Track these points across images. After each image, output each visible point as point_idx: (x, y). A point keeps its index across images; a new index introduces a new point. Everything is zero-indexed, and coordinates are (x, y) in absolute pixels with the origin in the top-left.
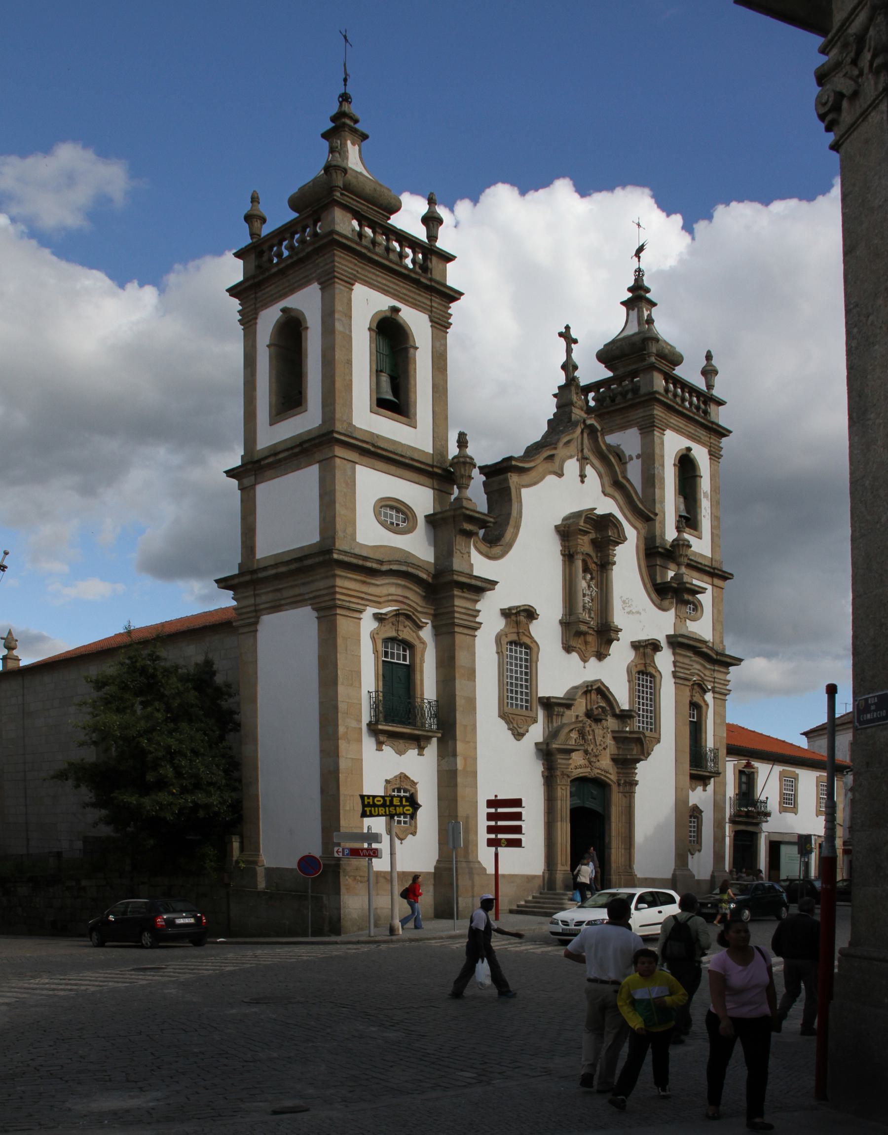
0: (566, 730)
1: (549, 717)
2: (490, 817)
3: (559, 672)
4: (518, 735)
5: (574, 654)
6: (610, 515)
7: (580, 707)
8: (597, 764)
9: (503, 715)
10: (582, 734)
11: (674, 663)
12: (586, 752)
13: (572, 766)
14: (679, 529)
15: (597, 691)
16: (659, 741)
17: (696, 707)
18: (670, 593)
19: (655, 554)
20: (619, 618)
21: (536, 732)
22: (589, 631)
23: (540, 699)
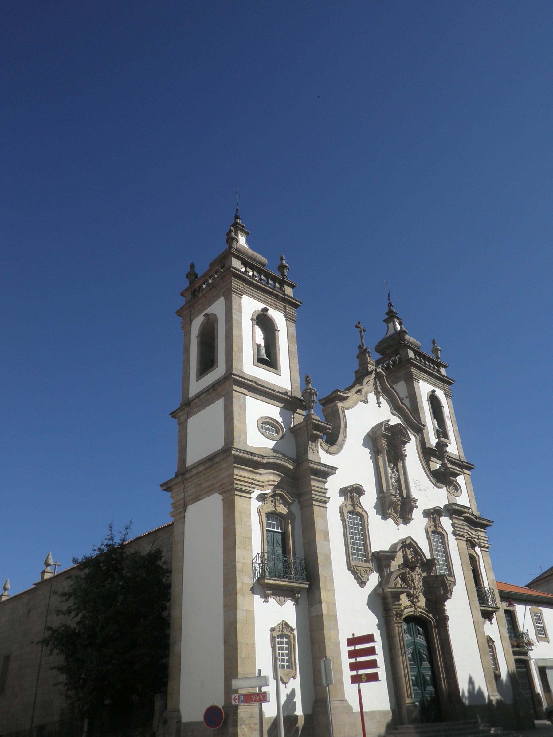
0: (394, 576)
1: (380, 570)
2: (352, 654)
3: (384, 534)
4: (362, 584)
5: (390, 520)
6: (399, 424)
7: (399, 560)
8: (418, 604)
9: (350, 568)
10: (404, 578)
11: (453, 525)
12: (409, 596)
13: (402, 607)
14: (438, 437)
15: (408, 545)
16: (454, 583)
17: (473, 560)
18: (443, 478)
19: (427, 453)
20: (414, 494)
21: (374, 579)
22: (397, 505)
23: (373, 554)
